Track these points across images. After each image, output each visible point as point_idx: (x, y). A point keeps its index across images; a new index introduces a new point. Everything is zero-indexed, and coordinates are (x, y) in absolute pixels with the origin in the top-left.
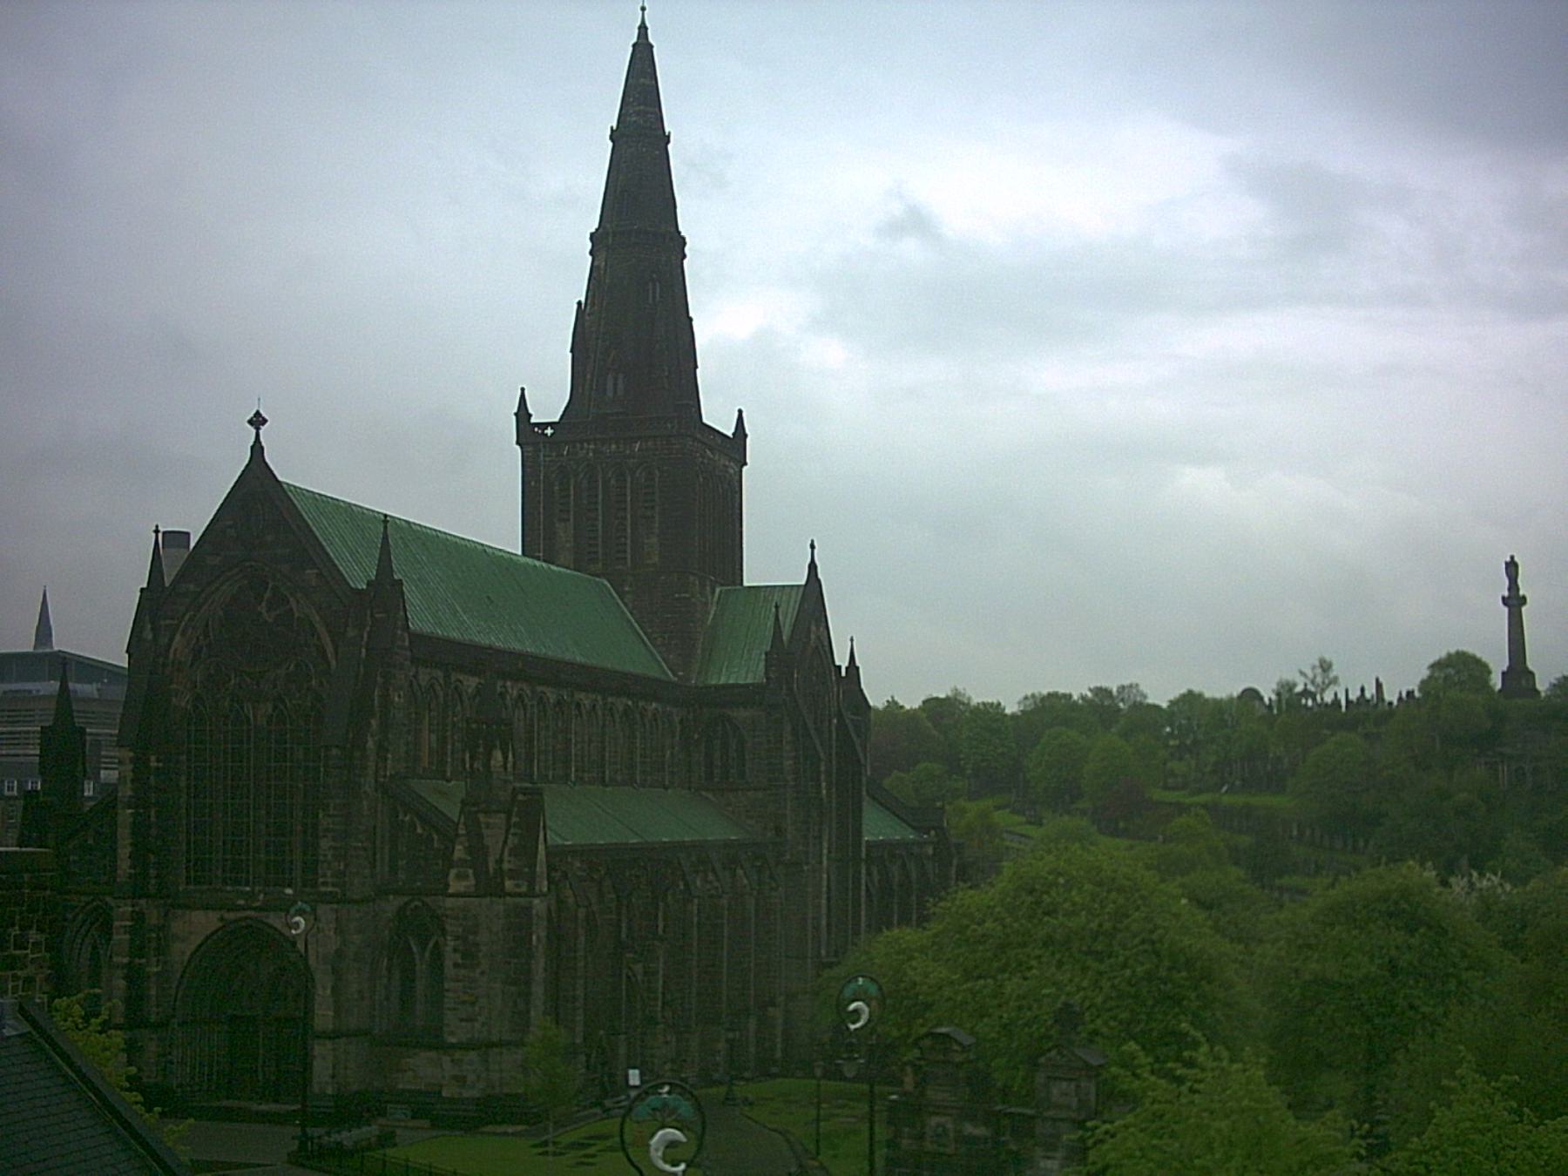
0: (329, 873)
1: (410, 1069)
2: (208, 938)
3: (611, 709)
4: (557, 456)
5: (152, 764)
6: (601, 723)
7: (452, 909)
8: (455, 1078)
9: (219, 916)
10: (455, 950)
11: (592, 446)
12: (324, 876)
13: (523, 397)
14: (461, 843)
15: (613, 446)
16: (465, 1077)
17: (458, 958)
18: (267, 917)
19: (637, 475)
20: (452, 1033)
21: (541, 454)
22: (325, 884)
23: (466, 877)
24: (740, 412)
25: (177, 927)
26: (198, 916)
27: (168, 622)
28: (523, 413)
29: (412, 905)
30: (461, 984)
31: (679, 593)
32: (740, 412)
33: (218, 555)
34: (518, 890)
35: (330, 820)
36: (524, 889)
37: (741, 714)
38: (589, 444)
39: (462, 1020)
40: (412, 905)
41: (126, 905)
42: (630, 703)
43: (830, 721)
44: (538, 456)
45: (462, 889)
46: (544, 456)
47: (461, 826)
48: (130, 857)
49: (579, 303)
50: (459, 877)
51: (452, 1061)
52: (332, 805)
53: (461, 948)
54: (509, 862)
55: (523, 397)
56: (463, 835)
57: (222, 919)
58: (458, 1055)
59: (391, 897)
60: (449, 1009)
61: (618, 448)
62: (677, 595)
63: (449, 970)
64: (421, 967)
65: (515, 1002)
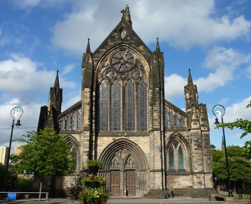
0: (157, 122)
1: (177, 182)
2: (109, 145)
5: (93, 94)
7: (193, 133)
8: (198, 182)
9: (113, 138)
10: (195, 145)
12: (155, 123)
14: (194, 115)
16: (202, 182)
17: (196, 147)
18: (129, 138)
20: (196, 169)
22: (156, 126)
23: (196, 124)
25: (99, 142)
26: (105, 139)
27: (96, 59)
29: (175, 134)
30: (198, 154)
33: (113, 42)
34: (205, 130)
35: (156, 108)
36: (206, 129)
39: (199, 165)
40: (175, 134)
41: (88, 133)
45: (196, 128)
47: (194, 110)
48: (88, 119)
50: (195, 124)
51: (197, 177)
52: (157, 103)
53: (197, 144)
54: (201, 122)
56: (195, 113)
57: (114, 139)
58: (198, 175)
59: (168, 132)
60: (195, 162)
63: (194, 151)
64: (176, 152)
65: (207, 161)
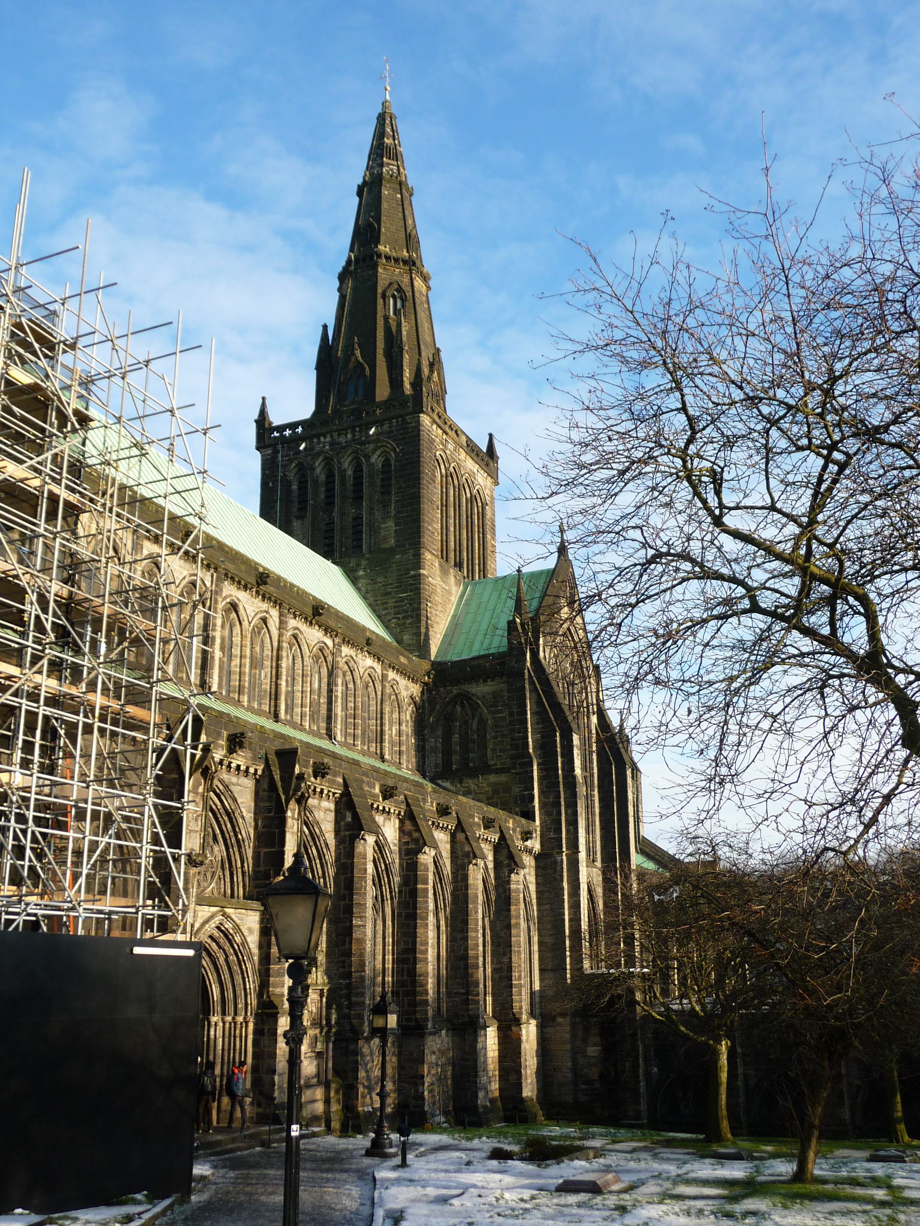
3: (295, 636)
4: (294, 454)
6: (275, 644)
11: (328, 439)
13: (264, 405)
15: (349, 436)
19: (373, 460)
21: (280, 455)
24: (491, 435)
28: (262, 422)
31: (413, 570)
32: (491, 435)
37: (481, 689)
38: (325, 438)
42: (329, 642)
43: (588, 717)
44: (277, 457)
46: (282, 456)
49: (325, 327)
55: (264, 405)
61: (354, 435)
62: (412, 572)
